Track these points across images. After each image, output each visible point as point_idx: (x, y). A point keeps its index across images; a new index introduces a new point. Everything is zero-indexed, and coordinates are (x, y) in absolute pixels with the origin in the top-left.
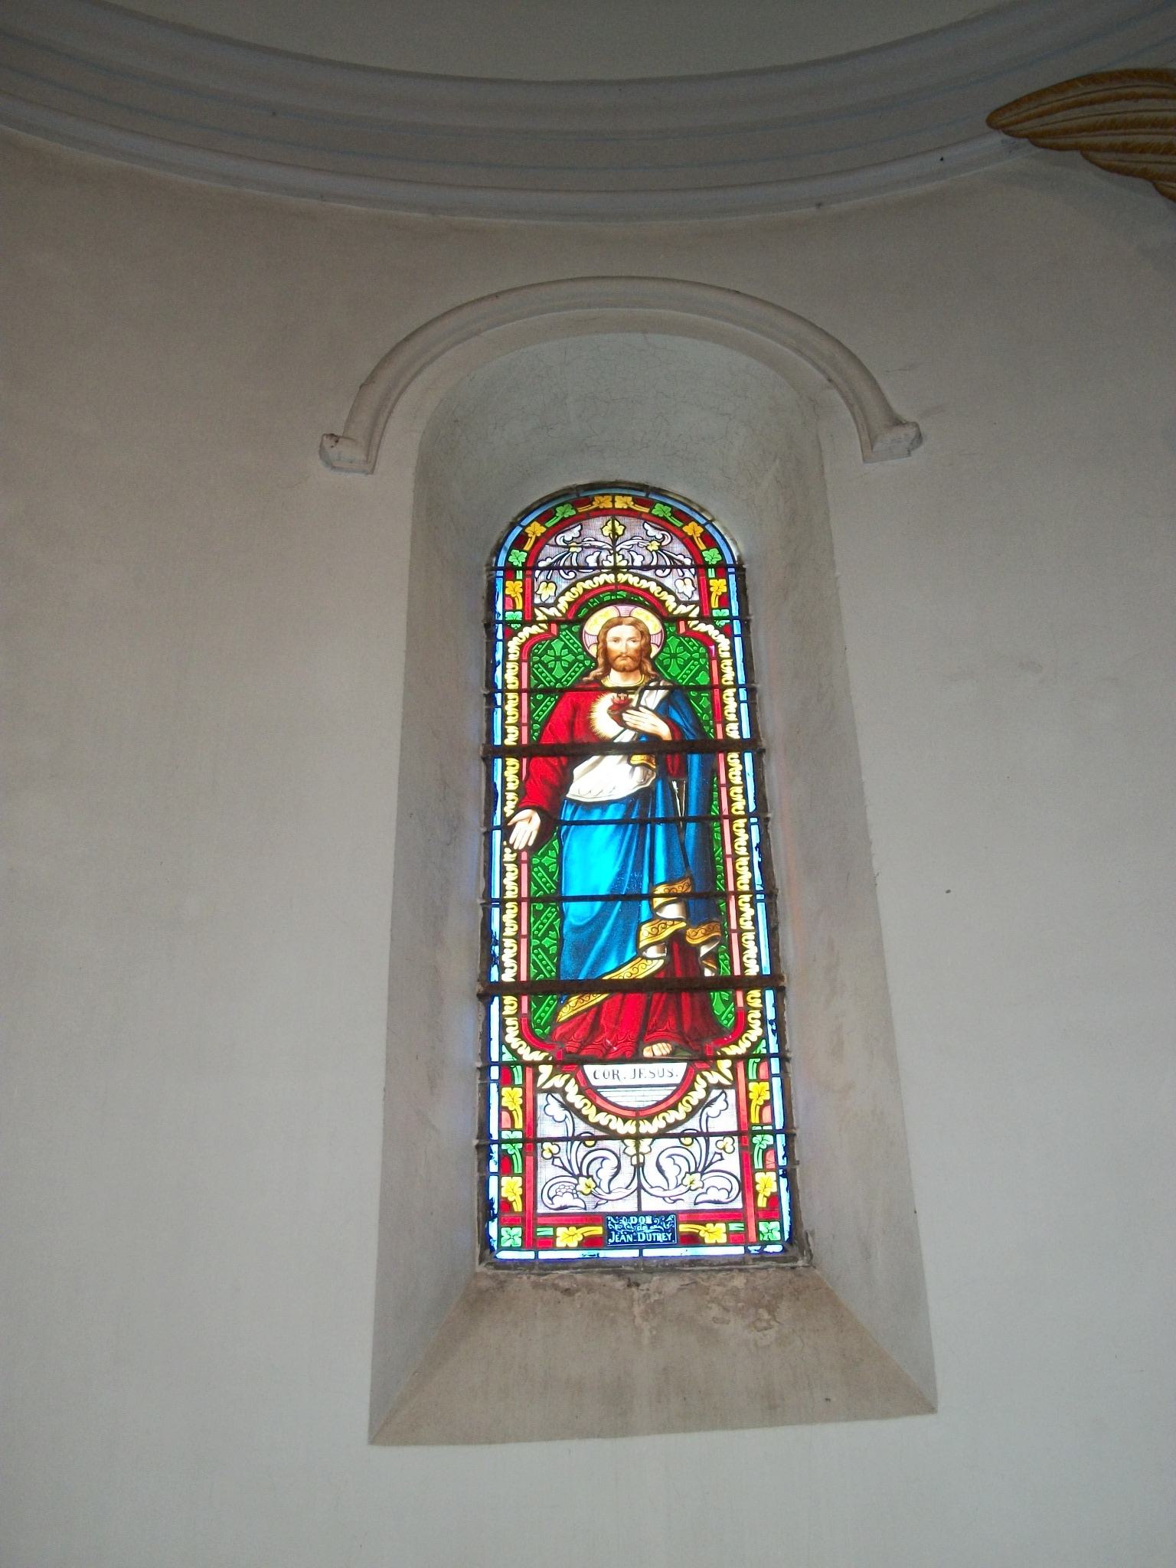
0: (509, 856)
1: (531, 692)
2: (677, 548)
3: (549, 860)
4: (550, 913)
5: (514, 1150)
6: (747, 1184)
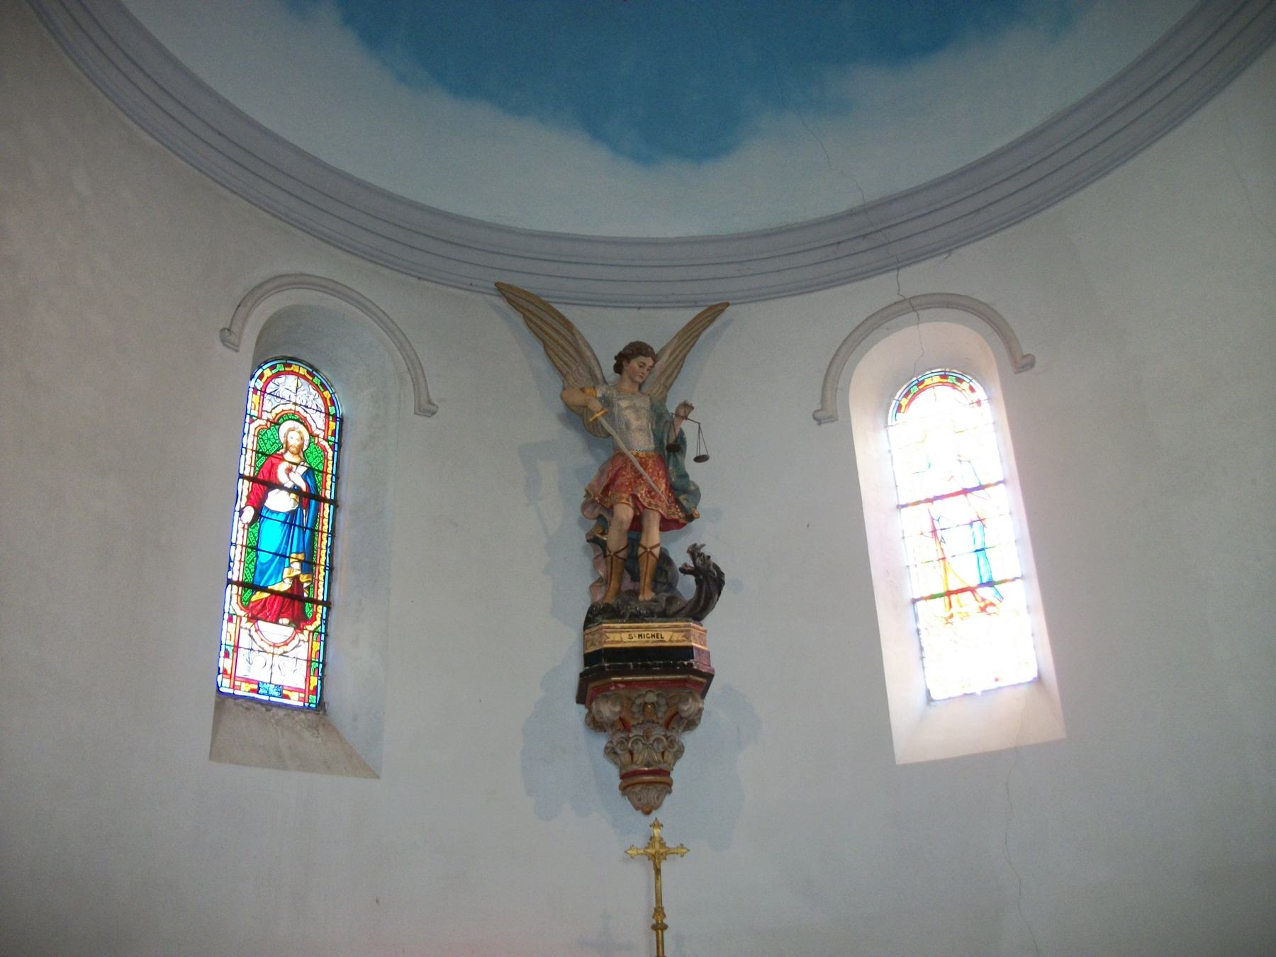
0: (241, 525)
1: (257, 452)
2: (320, 402)
3: (255, 531)
4: (253, 554)
5: (230, 649)
6: (307, 680)
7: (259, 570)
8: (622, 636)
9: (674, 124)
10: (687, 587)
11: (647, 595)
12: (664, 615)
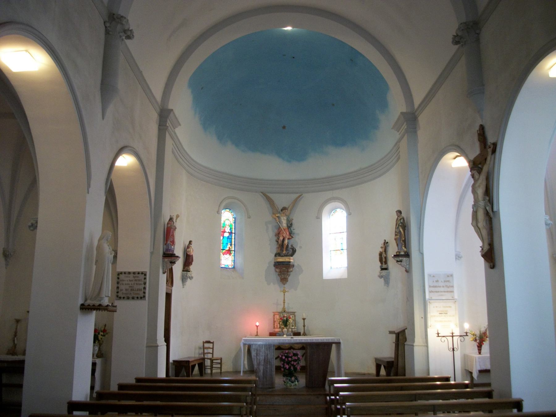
7: (224, 247)
8: (281, 259)
9: (295, 153)
10: (291, 252)
11: (284, 252)
12: (287, 256)
